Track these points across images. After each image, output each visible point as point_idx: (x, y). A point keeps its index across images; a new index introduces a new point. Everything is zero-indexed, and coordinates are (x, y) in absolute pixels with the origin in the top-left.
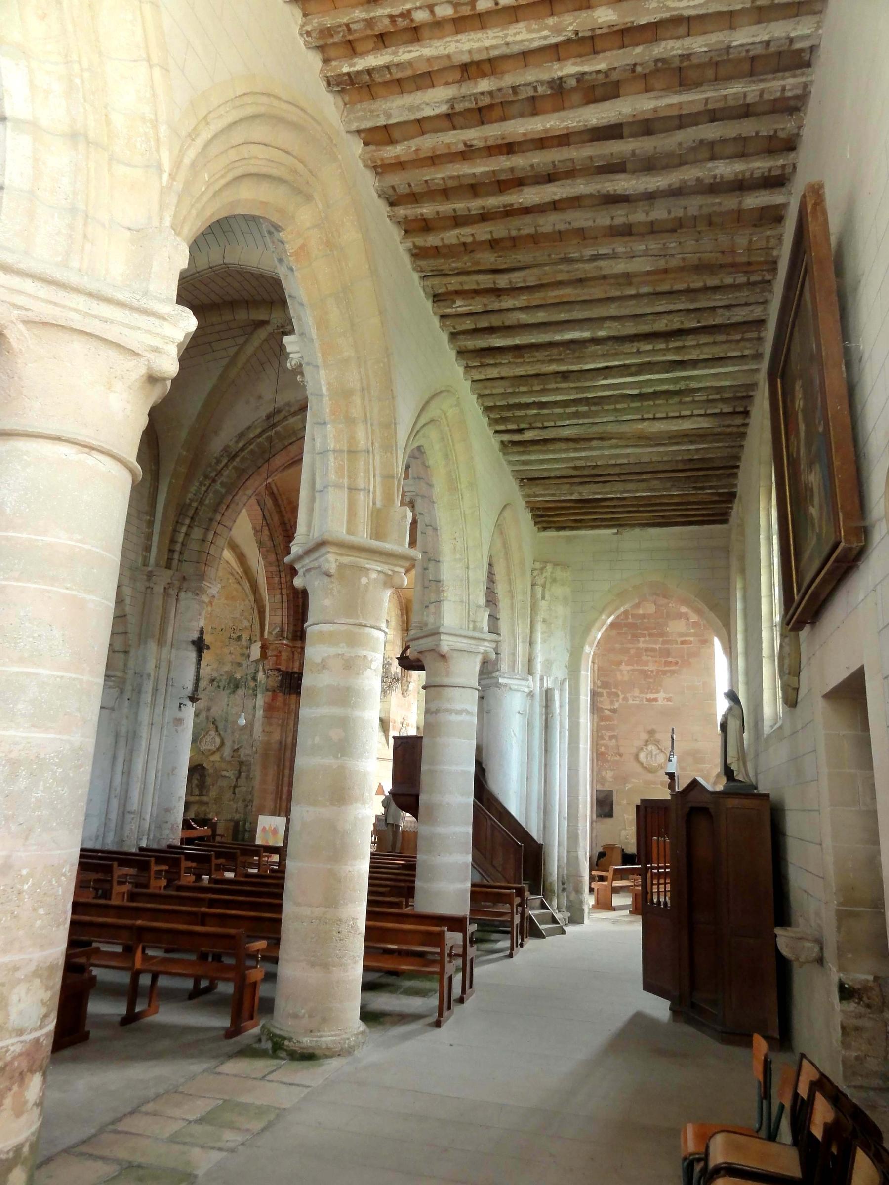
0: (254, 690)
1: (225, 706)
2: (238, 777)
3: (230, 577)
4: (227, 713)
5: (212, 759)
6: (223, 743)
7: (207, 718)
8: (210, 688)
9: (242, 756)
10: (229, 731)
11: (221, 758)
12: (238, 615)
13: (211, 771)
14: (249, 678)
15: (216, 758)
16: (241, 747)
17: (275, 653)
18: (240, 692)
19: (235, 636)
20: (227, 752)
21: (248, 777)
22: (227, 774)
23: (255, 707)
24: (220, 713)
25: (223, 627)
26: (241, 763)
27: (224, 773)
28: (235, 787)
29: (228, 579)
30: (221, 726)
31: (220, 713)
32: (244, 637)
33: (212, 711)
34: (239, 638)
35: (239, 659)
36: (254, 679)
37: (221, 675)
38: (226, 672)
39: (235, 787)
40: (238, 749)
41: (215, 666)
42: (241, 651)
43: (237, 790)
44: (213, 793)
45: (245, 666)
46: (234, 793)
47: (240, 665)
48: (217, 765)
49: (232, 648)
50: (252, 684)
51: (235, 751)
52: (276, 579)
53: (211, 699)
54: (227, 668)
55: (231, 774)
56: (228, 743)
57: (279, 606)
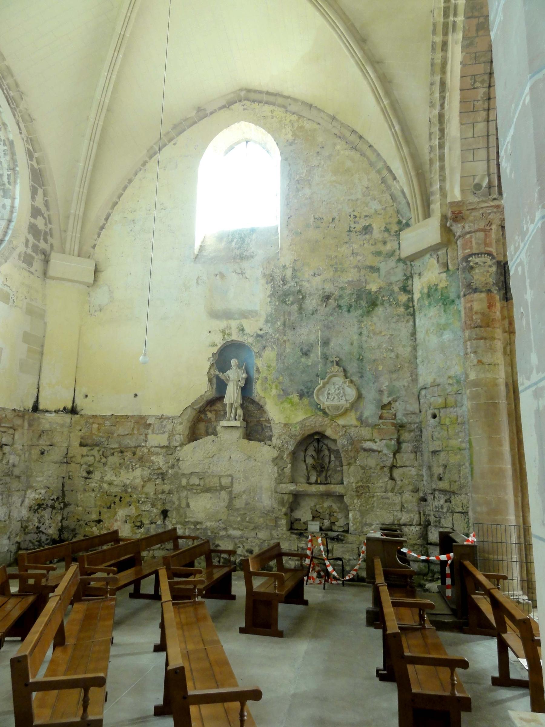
0: (407, 307)
1: (356, 337)
2: (397, 451)
3: (338, 141)
4: (361, 347)
5: (341, 422)
6: (360, 396)
7: (325, 357)
8: (323, 310)
9: (399, 416)
10: (368, 375)
11: (359, 419)
12: (359, 196)
13: (342, 442)
14: (396, 289)
15: (351, 419)
16: (395, 400)
17: (482, 225)
18: (380, 310)
19: (359, 227)
20: (369, 410)
21: (417, 451)
22: (374, 446)
23: (414, 334)
24: (347, 348)
25: (335, 215)
26: (400, 427)
27: (368, 445)
28: (393, 467)
29: (335, 145)
30: (352, 367)
31: (347, 348)
32: (375, 226)
33: (332, 344)
34: (367, 229)
35: (371, 260)
36: (406, 289)
37: (342, 289)
38: (349, 283)
39: (393, 467)
40: (390, 403)
41: (329, 274)
42: (373, 249)
43: (397, 473)
44: (351, 477)
45: (383, 272)
46: (392, 478)
47: (374, 269)
48: (353, 432)
49: (355, 246)
50: (403, 298)
51: (383, 407)
52: (481, 92)
53: (328, 327)
54: (351, 275)
55: (383, 445)
56: (370, 394)
57: (482, 143)
